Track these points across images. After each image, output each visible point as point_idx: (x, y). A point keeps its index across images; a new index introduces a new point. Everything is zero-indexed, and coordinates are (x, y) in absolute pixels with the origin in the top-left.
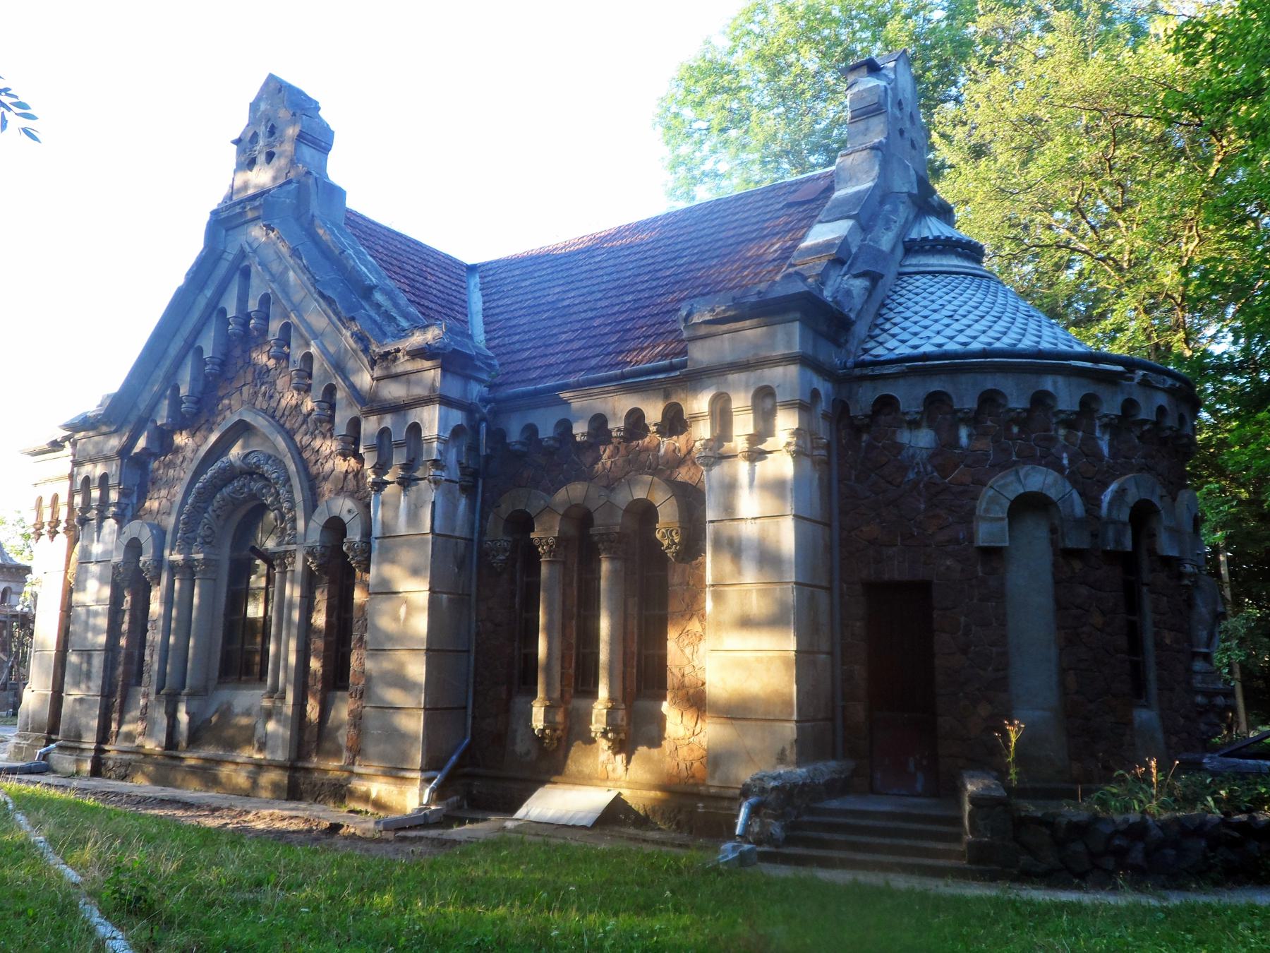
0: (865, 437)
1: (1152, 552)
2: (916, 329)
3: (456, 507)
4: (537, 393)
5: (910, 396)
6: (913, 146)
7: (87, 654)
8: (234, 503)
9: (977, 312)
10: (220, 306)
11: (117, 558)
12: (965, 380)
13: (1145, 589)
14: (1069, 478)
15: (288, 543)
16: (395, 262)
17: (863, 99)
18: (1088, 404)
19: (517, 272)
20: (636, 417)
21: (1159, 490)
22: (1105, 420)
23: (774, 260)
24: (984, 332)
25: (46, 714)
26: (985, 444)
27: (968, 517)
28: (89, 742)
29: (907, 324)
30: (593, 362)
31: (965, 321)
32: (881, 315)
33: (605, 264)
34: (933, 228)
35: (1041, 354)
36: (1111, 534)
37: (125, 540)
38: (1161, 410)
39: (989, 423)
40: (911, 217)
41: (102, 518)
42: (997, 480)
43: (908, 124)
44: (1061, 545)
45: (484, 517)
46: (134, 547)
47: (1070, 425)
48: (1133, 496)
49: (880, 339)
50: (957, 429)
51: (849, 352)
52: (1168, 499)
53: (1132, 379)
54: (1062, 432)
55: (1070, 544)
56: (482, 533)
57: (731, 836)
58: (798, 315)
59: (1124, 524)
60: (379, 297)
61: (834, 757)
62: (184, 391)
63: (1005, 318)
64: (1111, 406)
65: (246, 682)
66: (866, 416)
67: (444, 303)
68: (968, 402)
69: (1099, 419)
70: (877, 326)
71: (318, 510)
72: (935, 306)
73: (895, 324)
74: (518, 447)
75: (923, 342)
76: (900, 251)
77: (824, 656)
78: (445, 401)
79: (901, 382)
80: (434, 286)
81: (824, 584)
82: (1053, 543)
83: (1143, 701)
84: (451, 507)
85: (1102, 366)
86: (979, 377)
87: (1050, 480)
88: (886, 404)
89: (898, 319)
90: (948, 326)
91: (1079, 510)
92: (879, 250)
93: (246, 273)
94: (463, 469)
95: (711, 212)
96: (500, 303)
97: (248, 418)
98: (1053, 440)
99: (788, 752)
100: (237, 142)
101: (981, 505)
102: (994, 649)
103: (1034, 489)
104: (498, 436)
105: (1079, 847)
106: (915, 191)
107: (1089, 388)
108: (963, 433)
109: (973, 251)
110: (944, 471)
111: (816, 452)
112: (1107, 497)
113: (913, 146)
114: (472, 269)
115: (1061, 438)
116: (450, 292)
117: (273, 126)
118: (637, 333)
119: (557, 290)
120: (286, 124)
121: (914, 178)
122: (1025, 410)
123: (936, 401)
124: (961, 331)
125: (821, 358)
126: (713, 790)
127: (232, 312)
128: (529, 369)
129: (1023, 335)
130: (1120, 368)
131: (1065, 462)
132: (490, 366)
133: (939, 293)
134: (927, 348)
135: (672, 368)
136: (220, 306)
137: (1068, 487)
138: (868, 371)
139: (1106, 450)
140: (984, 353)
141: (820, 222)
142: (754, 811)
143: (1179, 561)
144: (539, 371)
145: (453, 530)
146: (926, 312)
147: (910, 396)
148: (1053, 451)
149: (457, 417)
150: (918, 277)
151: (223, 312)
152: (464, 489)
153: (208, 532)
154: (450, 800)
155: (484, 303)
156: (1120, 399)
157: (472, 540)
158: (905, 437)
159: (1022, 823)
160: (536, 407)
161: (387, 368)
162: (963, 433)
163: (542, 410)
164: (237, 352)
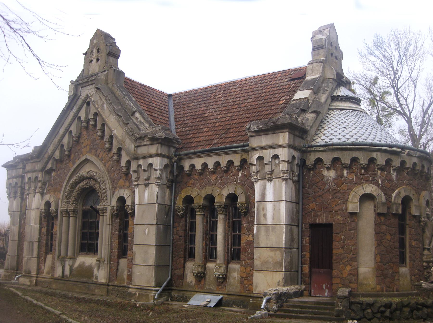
0: (312, 172)
1: (410, 213)
2: (332, 132)
3: (165, 193)
4: (195, 153)
5: (327, 158)
6: (336, 58)
7: (31, 242)
8: (83, 190)
9: (355, 126)
10: (79, 115)
11: (42, 207)
12: (346, 153)
13: (407, 226)
14: (381, 188)
15: (104, 205)
16: (142, 98)
17: (317, 42)
18: (388, 162)
19: (188, 99)
20: (231, 163)
21: (413, 192)
22: (394, 168)
23: (283, 104)
24: (356, 134)
25: (15, 263)
26: (352, 176)
27: (346, 201)
28: (34, 272)
29: (329, 130)
30: (215, 141)
31: (349, 129)
32: (320, 126)
33: (221, 99)
34: (343, 91)
35: (372, 145)
36: (394, 207)
37: (44, 202)
38: (415, 164)
39: (354, 168)
40: (334, 87)
41: (35, 193)
42: (356, 189)
43: (334, 51)
44: (377, 212)
45: (175, 198)
46: (48, 204)
47: (382, 169)
48: (403, 195)
49: (319, 136)
50: (343, 170)
51: (307, 141)
52: (416, 195)
53: (404, 153)
54: (379, 172)
55: (380, 211)
56: (175, 203)
57: (260, 309)
58: (287, 130)
59: (399, 204)
61: (298, 284)
62: (65, 147)
63: (364, 128)
64: (396, 163)
65: (89, 254)
66: (312, 165)
67: (160, 114)
68: (346, 161)
69: (392, 167)
70: (319, 130)
71: (116, 194)
72: (340, 123)
73: (325, 130)
74: (188, 172)
75: (334, 137)
76: (329, 100)
77: (295, 249)
78: (162, 156)
79: (324, 153)
80: (156, 106)
81: (297, 224)
82: (375, 210)
84: (164, 193)
86: (351, 152)
87: (374, 189)
88: (319, 161)
89: (326, 128)
90: (343, 131)
91: (384, 199)
92: (320, 102)
93: (88, 104)
94: (168, 180)
95: (262, 80)
96: (181, 113)
97: (89, 158)
98: (375, 174)
99: (281, 282)
100: (84, 54)
101: (350, 198)
102: (352, 247)
104: (181, 168)
105: (369, 311)
106: (336, 78)
108: (345, 172)
109: (357, 101)
110: (338, 185)
111: (294, 178)
112: (394, 195)
113: (336, 58)
114: (170, 96)
115: (379, 174)
116: (161, 108)
117: (99, 49)
118: (232, 130)
119: (202, 109)
120: (104, 48)
121: (335, 73)
122: (366, 164)
123: (336, 160)
124: (348, 133)
125: (296, 144)
126: (255, 295)
127: (83, 118)
128: (192, 142)
129: (370, 135)
130: (399, 150)
131: (380, 182)
132: (178, 142)
133: (342, 118)
134: (335, 141)
135: (244, 146)
136: (79, 115)
137: (380, 191)
138: (313, 149)
139: (394, 178)
140: (353, 144)
141: (300, 90)
142: (268, 301)
143: (420, 217)
144: (195, 143)
145: (164, 202)
146: (336, 125)
147: (327, 158)
148: (376, 178)
149: (166, 161)
150: (335, 111)
151: (80, 118)
152: (168, 187)
153: (74, 200)
154: (164, 298)
155: (175, 112)
156: (400, 160)
157: (171, 206)
158: (325, 172)
159: (351, 303)
160: (195, 158)
161: (141, 142)
162: (345, 172)
163: (197, 159)
164: (84, 133)
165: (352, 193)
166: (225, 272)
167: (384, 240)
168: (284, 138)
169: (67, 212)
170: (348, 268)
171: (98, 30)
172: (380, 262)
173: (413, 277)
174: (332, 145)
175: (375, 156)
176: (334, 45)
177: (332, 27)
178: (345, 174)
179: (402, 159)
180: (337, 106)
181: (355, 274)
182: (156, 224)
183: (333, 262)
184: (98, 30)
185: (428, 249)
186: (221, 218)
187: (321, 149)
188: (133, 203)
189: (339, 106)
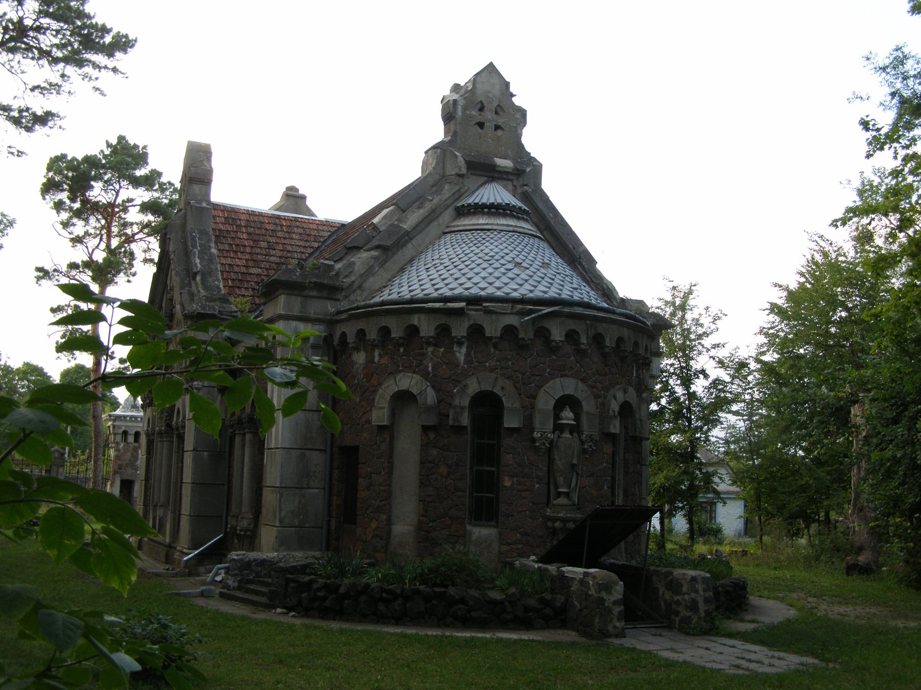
18: (444, 331)
26: (384, 361)
54: (430, 349)
58: (280, 291)
59: (463, 408)
60: (198, 278)
61: (321, 550)
64: (460, 329)
83: (493, 523)
85: (450, 305)
87: (413, 382)
103: (403, 388)
107: (443, 320)
108: (377, 353)
130: (463, 304)
131: (430, 369)
139: (462, 359)
159: (288, 581)
162: (377, 353)
165: (380, 391)
166: (252, 527)
167: (433, 476)
168: (281, 304)
169: (160, 433)
170: (374, 525)
171: (189, 142)
172: (423, 516)
173: (505, 548)
174: (358, 308)
175: (416, 322)
176: (490, 106)
178: (377, 358)
179: (472, 322)
180: (458, 226)
181: (387, 536)
182: (194, 450)
183: (358, 513)
184: (189, 142)
185: (567, 495)
186: (248, 437)
187: (344, 316)
188: (184, 418)
189: (458, 226)
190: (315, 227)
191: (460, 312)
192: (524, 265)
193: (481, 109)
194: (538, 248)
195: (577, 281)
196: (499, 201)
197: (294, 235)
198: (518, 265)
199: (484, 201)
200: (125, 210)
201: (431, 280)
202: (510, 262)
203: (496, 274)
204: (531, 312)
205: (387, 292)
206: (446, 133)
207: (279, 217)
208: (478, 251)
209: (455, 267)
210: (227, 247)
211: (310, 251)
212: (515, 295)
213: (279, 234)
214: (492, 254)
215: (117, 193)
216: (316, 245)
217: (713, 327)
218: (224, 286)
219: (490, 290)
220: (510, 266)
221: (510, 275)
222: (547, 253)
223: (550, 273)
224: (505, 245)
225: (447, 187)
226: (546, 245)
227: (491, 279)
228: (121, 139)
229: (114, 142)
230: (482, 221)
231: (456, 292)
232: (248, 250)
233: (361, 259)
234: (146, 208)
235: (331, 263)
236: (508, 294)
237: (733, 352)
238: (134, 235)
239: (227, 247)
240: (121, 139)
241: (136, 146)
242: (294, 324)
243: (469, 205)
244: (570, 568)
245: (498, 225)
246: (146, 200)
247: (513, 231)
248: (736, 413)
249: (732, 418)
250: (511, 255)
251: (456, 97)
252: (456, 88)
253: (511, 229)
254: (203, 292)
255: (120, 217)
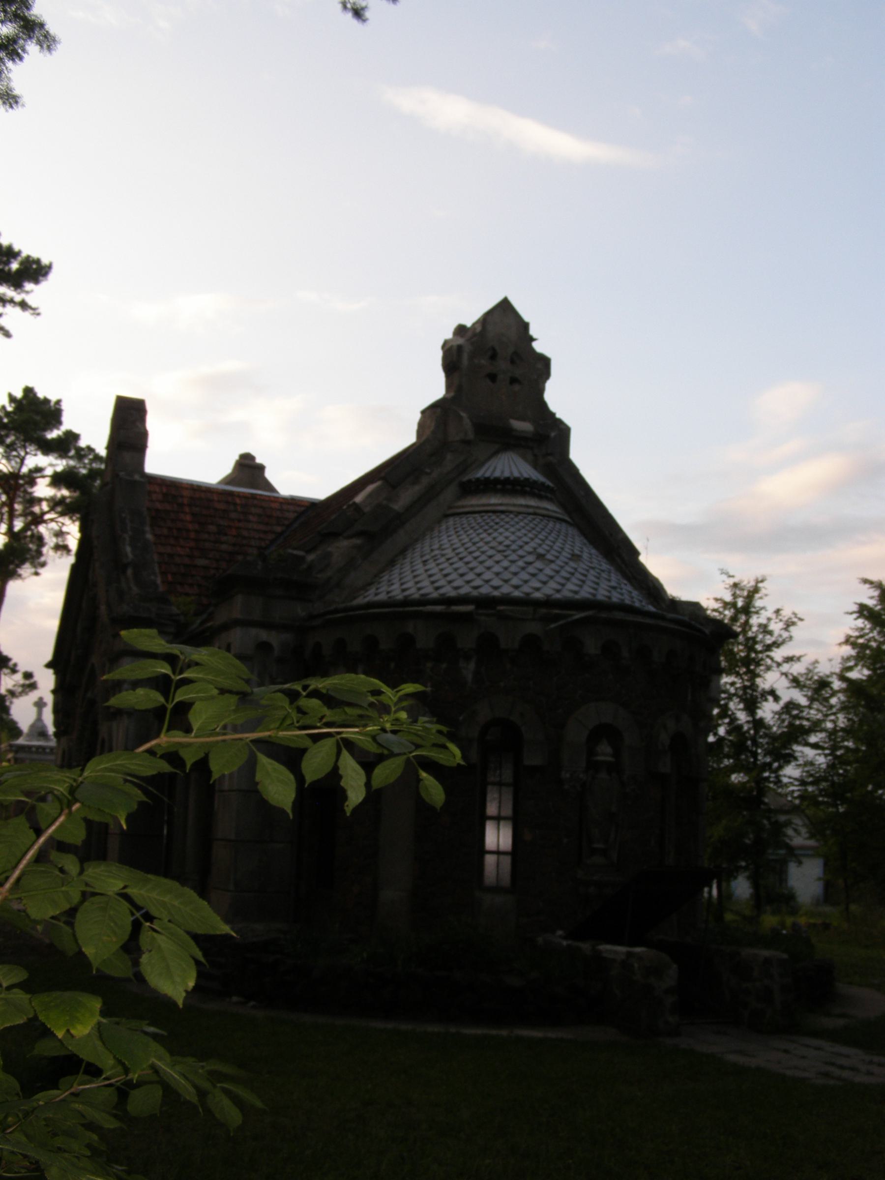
54: (429, 665)
60: (130, 572)
85: (455, 608)
130: (470, 608)
139: (470, 677)
174: (336, 611)
177: (505, 306)
180: (463, 507)
189: (463, 507)
190: (276, 506)
191: (466, 618)
192: (549, 557)
193: (494, 356)
194: (566, 536)
195: (615, 578)
196: (516, 474)
197: (251, 518)
198: (541, 557)
199: (497, 474)
200: (32, 482)
201: (430, 576)
202: (530, 553)
203: (513, 569)
204: (557, 618)
205: (372, 591)
206: (449, 386)
207: (231, 494)
208: (489, 539)
209: (461, 559)
210: (165, 531)
211: (271, 537)
212: (537, 595)
213: (233, 515)
214: (507, 542)
215: (23, 460)
216: (279, 529)
217: (785, 635)
218: (163, 582)
219: (506, 589)
220: (530, 558)
221: (531, 569)
222: (576, 542)
223: (582, 567)
224: (523, 531)
225: (449, 456)
226: (572, 531)
227: (506, 575)
228: (29, 392)
229: (19, 394)
230: (494, 500)
231: (463, 591)
232: (192, 535)
233: (340, 548)
234: (58, 480)
235: (300, 553)
236: (528, 594)
237: (811, 667)
238: (43, 513)
239: (165, 531)
240: (29, 392)
241: (46, 401)
242: (253, 631)
243: (478, 480)
244: (609, 947)
245: (514, 505)
246: (59, 469)
247: (535, 514)
248: (815, 746)
249: (810, 753)
250: (533, 544)
251: (460, 341)
252: (461, 330)
253: (531, 510)
254: (135, 590)
255: (25, 492)
